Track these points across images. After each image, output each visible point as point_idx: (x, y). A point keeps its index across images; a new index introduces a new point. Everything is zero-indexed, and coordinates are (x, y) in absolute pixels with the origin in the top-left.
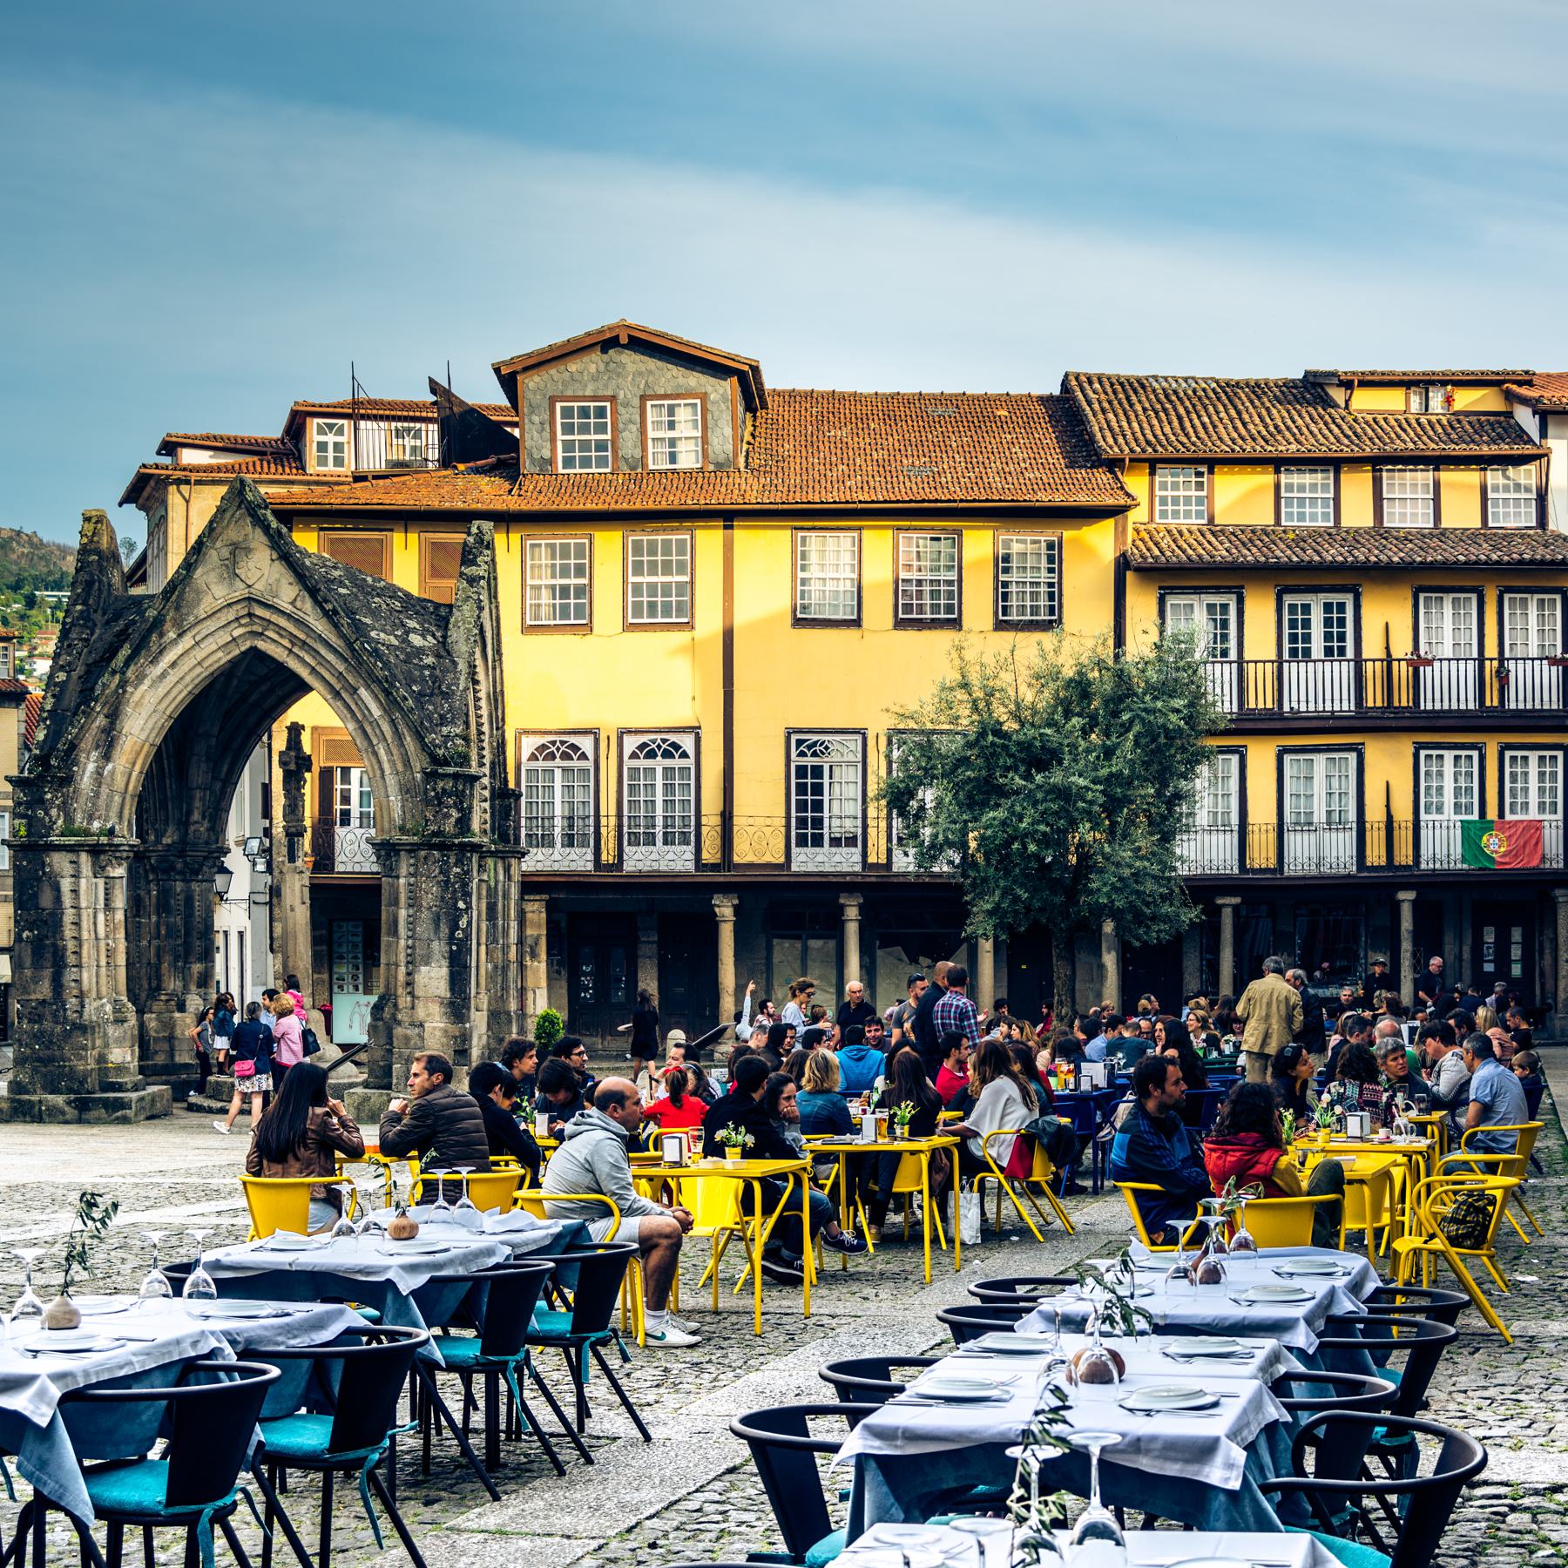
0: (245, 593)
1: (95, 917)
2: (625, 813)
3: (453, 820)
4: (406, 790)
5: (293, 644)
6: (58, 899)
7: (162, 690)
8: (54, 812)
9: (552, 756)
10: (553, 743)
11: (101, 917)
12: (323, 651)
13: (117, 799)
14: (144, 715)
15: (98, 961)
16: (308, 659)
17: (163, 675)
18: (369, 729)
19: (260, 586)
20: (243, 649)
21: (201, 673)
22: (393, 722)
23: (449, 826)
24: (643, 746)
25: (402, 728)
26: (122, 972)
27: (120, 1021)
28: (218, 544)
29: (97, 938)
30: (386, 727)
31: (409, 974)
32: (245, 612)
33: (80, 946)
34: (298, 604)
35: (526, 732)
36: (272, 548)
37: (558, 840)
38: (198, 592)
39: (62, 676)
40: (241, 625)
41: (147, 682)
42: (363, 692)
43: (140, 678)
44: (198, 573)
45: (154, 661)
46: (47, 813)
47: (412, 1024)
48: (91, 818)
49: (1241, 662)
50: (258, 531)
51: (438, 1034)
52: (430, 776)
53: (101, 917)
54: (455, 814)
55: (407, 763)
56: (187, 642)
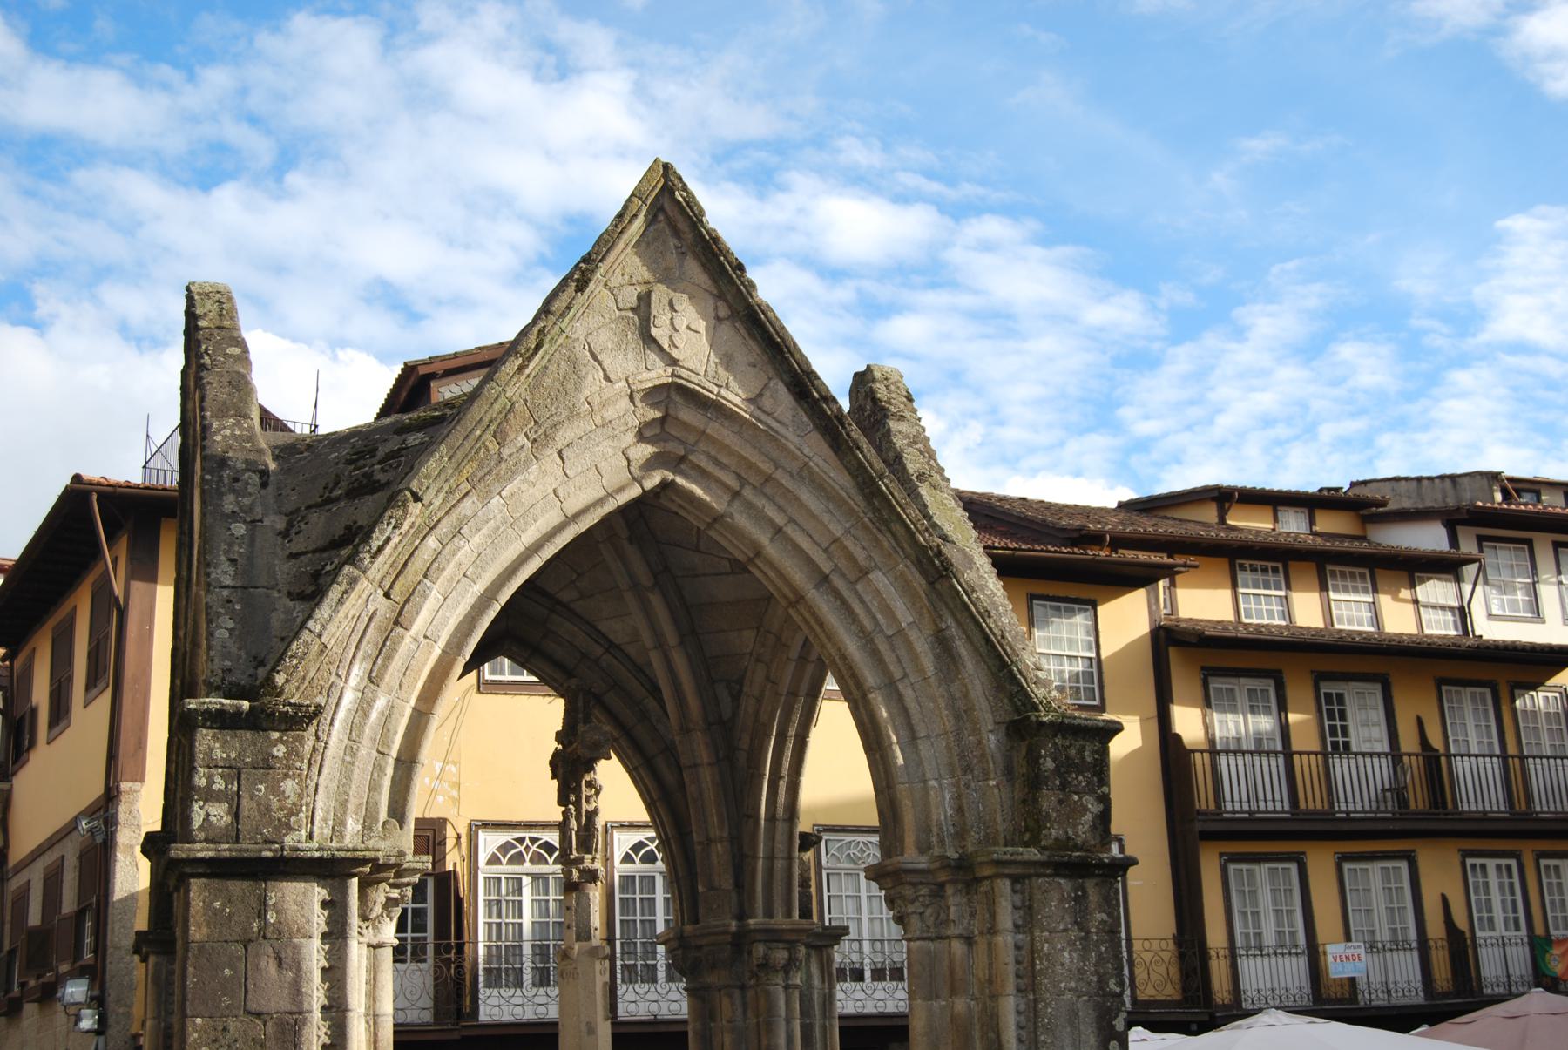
2: (618, 935)
3: (1088, 817)
5: (743, 481)
6: (297, 989)
8: (289, 786)
9: (518, 859)
10: (521, 840)
12: (806, 496)
16: (771, 511)
18: (883, 647)
22: (942, 642)
23: (1083, 829)
24: (637, 847)
25: (962, 649)
30: (921, 644)
34: (767, 403)
35: (486, 825)
36: (720, 296)
37: (527, 977)
42: (878, 578)
46: (276, 790)
49: (1288, 754)
54: (1094, 807)
55: (962, 714)
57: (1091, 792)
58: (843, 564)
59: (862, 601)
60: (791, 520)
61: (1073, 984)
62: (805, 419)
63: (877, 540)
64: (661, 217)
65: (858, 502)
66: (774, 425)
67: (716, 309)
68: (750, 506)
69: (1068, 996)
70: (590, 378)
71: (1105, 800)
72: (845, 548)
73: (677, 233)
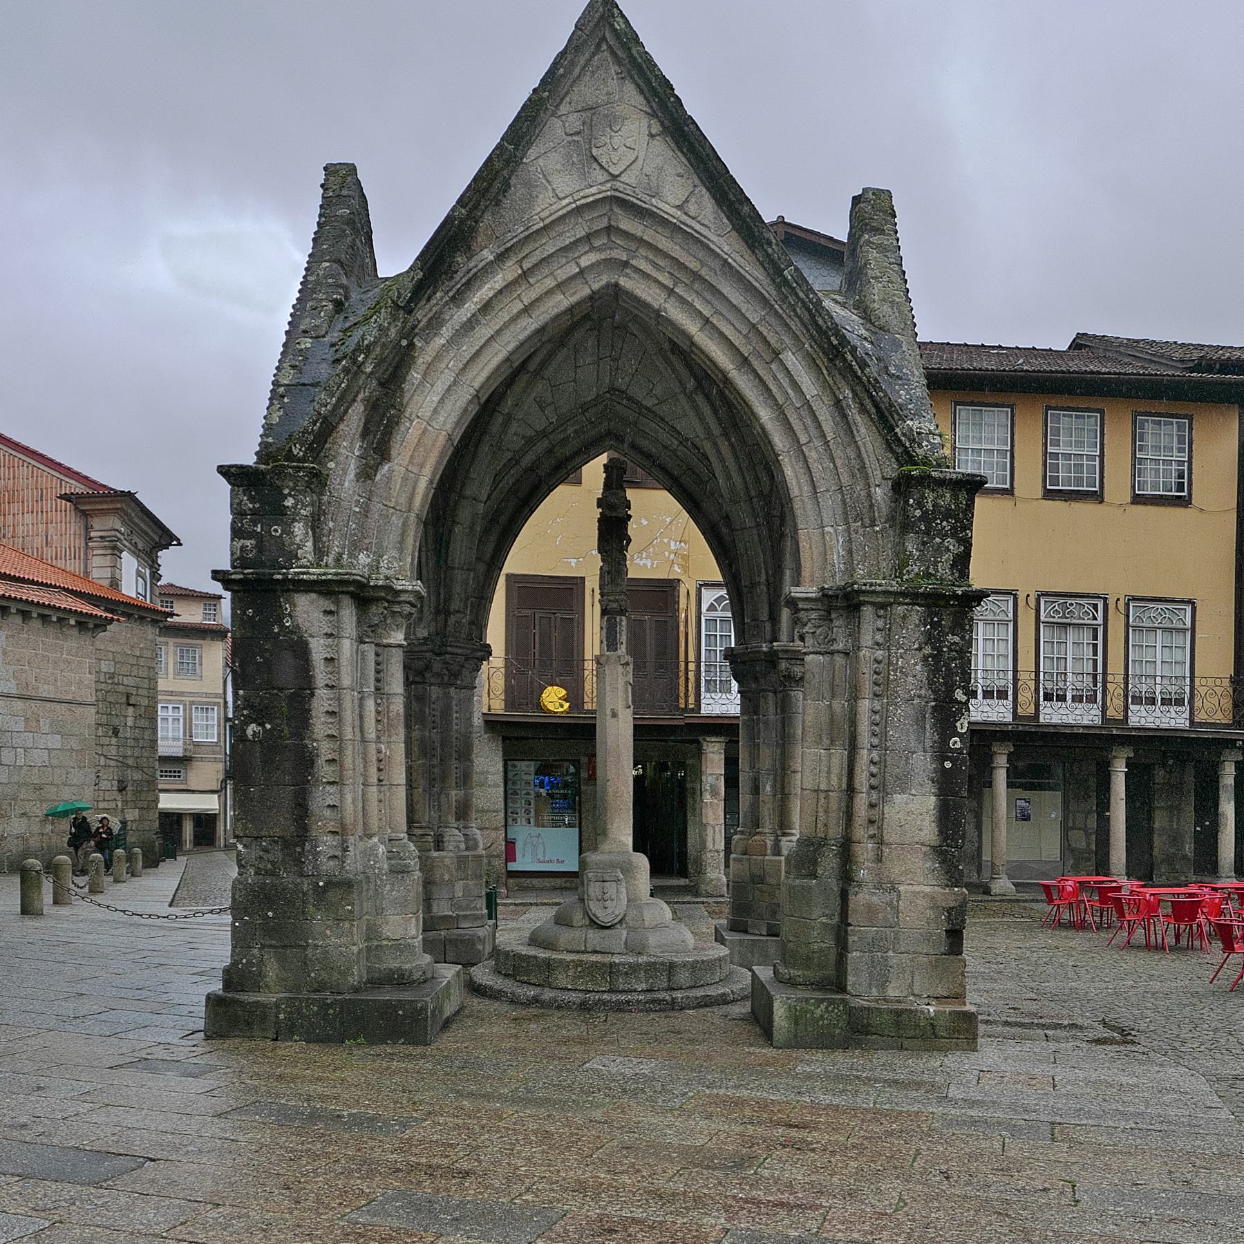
0: (607, 190)
1: (361, 706)
4: (855, 513)
5: (677, 281)
7: (467, 349)
11: (370, 705)
12: (727, 289)
13: (396, 521)
14: (440, 387)
15: (365, 776)
17: (470, 325)
19: (630, 178)
20: (596, 286)
21: (529, 325)
26: (401, 793)
27: (399, 871)
28: (564, 109)
29: (364, 740)
31: (872, 806)
32: (604, 223)
33: (341, 751)
34: (692, 208)
36: (654, 115)
38: (529, 185)
39: (307, 343)
40: (592, 249)
41: (446, 332)
42: (790, 358)
43: (436, 323)
44: (532, 153)
45: (458, 299)
47: (879, 886)
48: (355, 548)
50: (630, 88)
51: (922, 903)
52: (901, 487)
53: (370, 705)
56: (509, 271)
57: (954, 535)
58: (761, 347)
59: (775, 378)
60: (717, 312)
61: (923, 692)
62: (725, 220)
63: (787, 325)
64: (604, 47)
65: (769, 291)
66: (698, 227)
67: (649, 127)
68: (683, 301)
69: (917, 701)
70: (541, 196)
71: (967, 543)
72: (761, 333)
73: (618, 60)
